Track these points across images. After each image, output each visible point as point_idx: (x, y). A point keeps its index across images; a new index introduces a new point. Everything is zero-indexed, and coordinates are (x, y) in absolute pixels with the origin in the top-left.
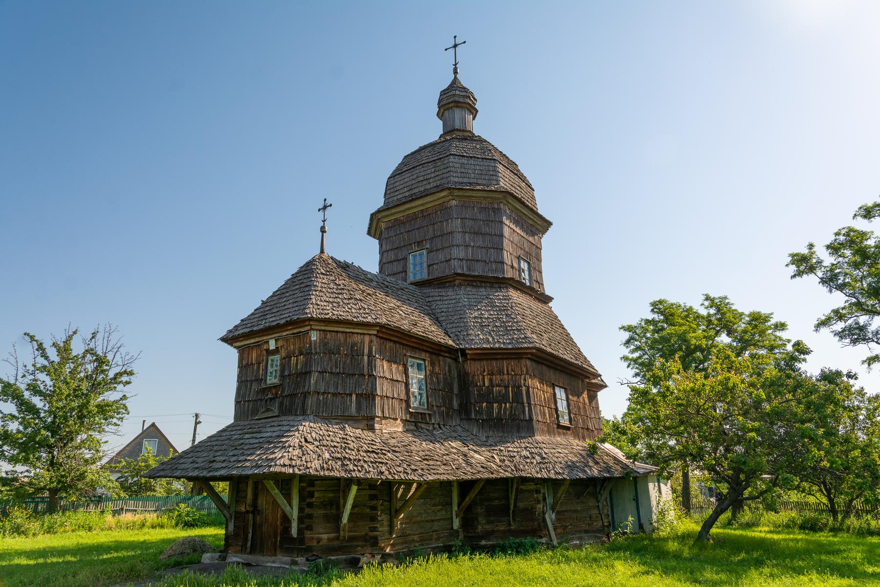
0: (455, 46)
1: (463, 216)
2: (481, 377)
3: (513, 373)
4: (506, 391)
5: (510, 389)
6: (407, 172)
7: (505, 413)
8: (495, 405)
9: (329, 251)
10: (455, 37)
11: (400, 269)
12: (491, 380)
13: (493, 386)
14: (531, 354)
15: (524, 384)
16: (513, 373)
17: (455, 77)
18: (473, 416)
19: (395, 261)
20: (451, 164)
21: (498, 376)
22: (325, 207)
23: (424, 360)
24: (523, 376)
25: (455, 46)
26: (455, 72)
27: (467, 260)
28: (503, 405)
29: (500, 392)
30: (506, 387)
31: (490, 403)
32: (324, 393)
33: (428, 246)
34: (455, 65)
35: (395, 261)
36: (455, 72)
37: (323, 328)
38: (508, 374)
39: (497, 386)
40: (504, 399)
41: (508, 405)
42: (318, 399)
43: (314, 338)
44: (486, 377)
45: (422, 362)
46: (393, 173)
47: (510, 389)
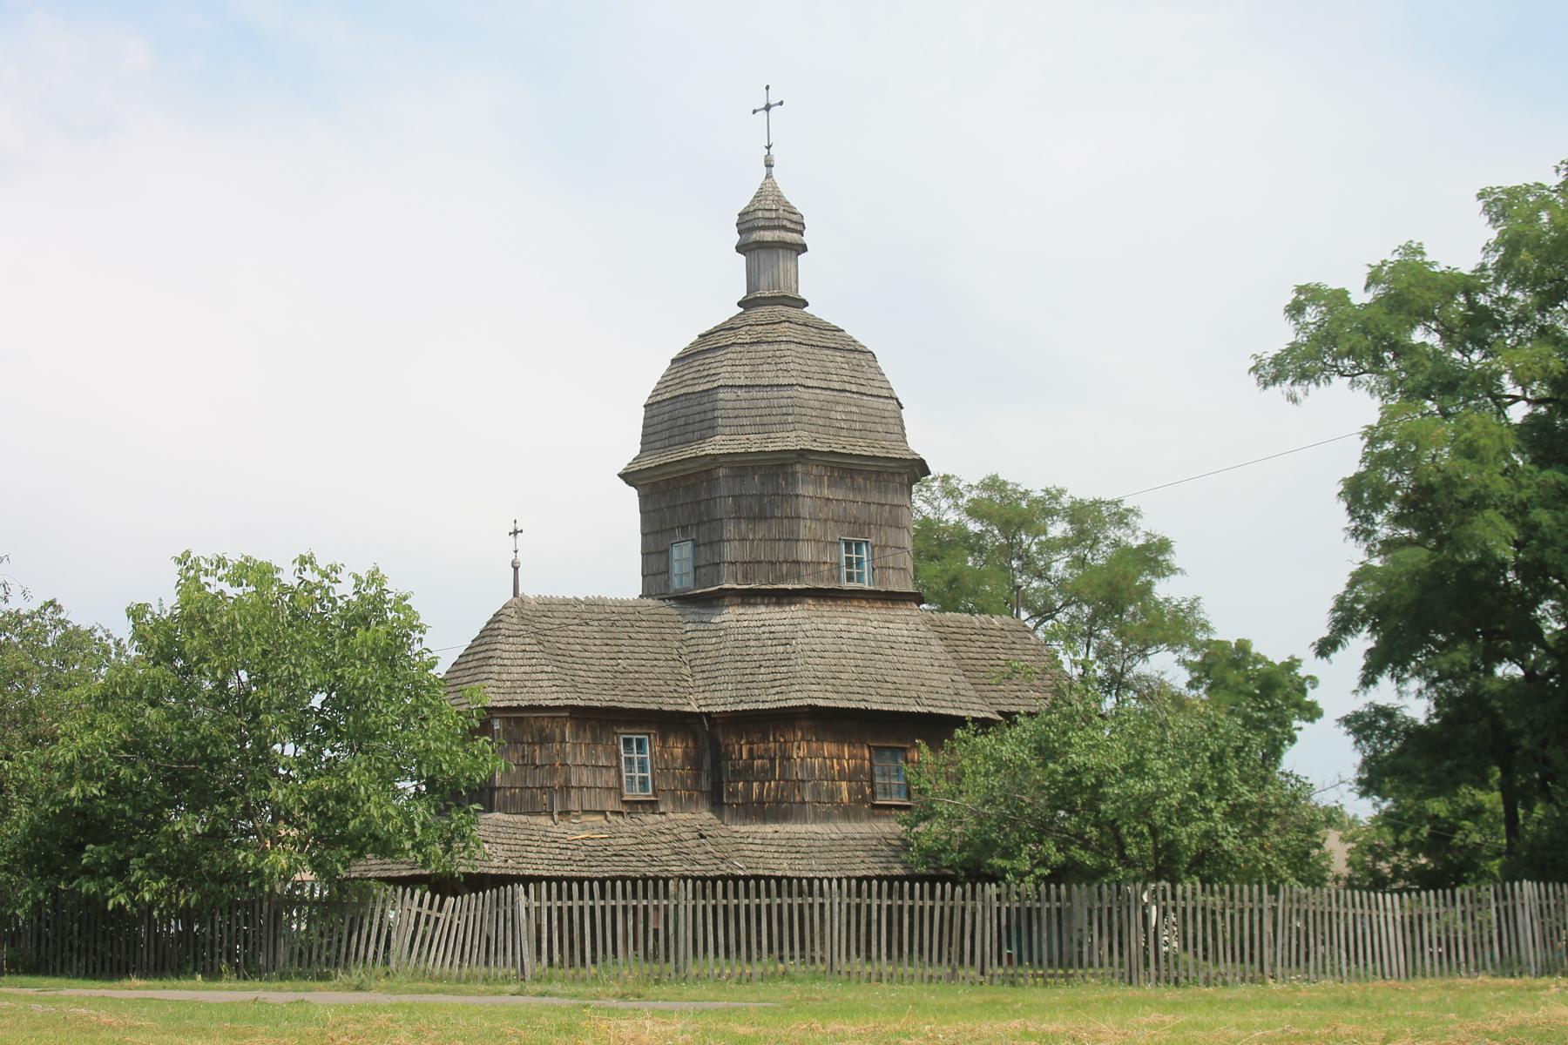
0: (768, 108)
1: (737, 492)
2: (737, 747)
3: (782, 740)
4: (771, 763)
5: (777, 762)
6: (667, 403)
7: (768, 795)
8: (755, 784)
9: (529, 590)
10: (767, 88)
11: (662, 568)
12: (751, 751)
13: (753, 759)
14: (806, 712)
15: (797, 754)
16: (782, 740)
17: (768, 176)
18: (725, 800)
19: (655, 552)
20: (720, 405)
21: (761, 745)
22: (516, 532)
23: (649, 735)
24: (796, 744)
25: (768, 108)
26: (769, 165)
27: (743, 563)
28: (767, 784)
29: (763, 766)
30: (772, 760)
31: (749, 783)
32: (511, 788)
33: (694, 537)
34: (768, 147)
35: (655, 552)
36: (769, 165)
37: (505, 715)
38: (775, 741)
39: (759, 758)
40: (766, 775)
41: (772, 783)
42: (505, 794)
43: (496, 728)
44: (744, 748)
45: (647, 737)
46: (656, 392)
47: (777, 762)
